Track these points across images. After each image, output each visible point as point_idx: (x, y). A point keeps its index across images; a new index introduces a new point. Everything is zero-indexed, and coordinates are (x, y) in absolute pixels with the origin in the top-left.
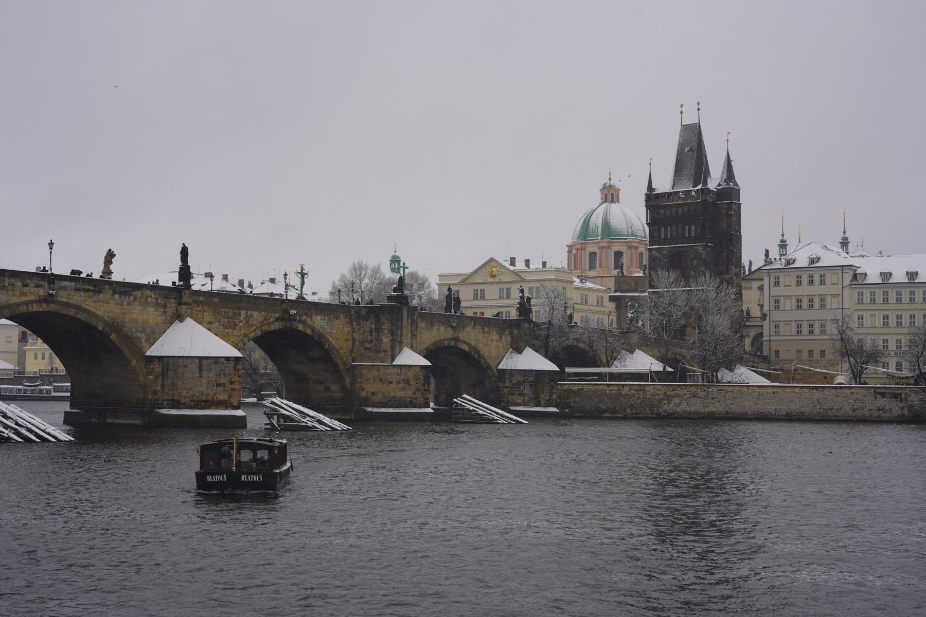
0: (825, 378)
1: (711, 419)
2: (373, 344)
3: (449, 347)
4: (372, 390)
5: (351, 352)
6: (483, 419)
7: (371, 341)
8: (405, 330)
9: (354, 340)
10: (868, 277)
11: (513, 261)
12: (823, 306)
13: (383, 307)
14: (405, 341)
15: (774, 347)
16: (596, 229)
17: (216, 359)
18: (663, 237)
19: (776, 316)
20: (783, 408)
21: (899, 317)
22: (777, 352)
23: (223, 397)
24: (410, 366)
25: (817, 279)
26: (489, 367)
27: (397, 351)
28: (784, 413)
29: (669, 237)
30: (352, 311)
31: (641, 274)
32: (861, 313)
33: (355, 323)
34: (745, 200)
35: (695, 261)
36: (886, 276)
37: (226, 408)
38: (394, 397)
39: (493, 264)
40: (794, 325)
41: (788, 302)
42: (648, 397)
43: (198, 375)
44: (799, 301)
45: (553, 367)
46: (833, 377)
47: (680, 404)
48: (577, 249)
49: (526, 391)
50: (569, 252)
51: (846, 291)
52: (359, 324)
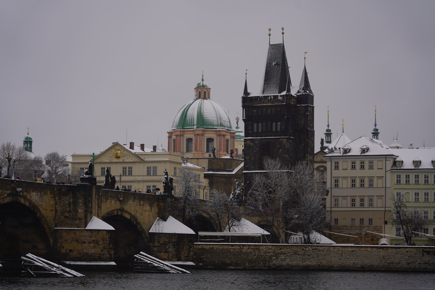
0: (372, 240)
1: (307, 270)
2: (71, 214)
3: (117, 215)
4: (70, 248)
5: (54, 219)
6: (158, 270)
7: (70, 212)
8: (93, 203)
9: (56, 210)
10: (404, 164)
11: (132, 145)
12: (371, 185)
13: (79, 186)
14: (94, 211)
15: (334, 216)
16: (192, 120)
18: (255, 130)
19: (336, 192)
20: (359, 262)
21: (426, 194)
22: (336, 220)
24: (99, 230)
25: (367, 165)
26: (143, 231)
27: (89, 219)
28: (360, 266)
29: (260, 130)
30: (55, 189)
31: (228, 157)
33: (57, 198)
34: (316, 104)
35: (281, 150)
36: (417, 163)
38: (87, 254)
39: (118, 147)
40: (349, 200)
41: (345, 181)
42: (262, 254)
44: (353, 181)
45: (190, 231)
46: (378, 240)
47: (285, 259)
48: (177, 136)
49: (170, 250)
50: (170, 137)
51: (388, 174)
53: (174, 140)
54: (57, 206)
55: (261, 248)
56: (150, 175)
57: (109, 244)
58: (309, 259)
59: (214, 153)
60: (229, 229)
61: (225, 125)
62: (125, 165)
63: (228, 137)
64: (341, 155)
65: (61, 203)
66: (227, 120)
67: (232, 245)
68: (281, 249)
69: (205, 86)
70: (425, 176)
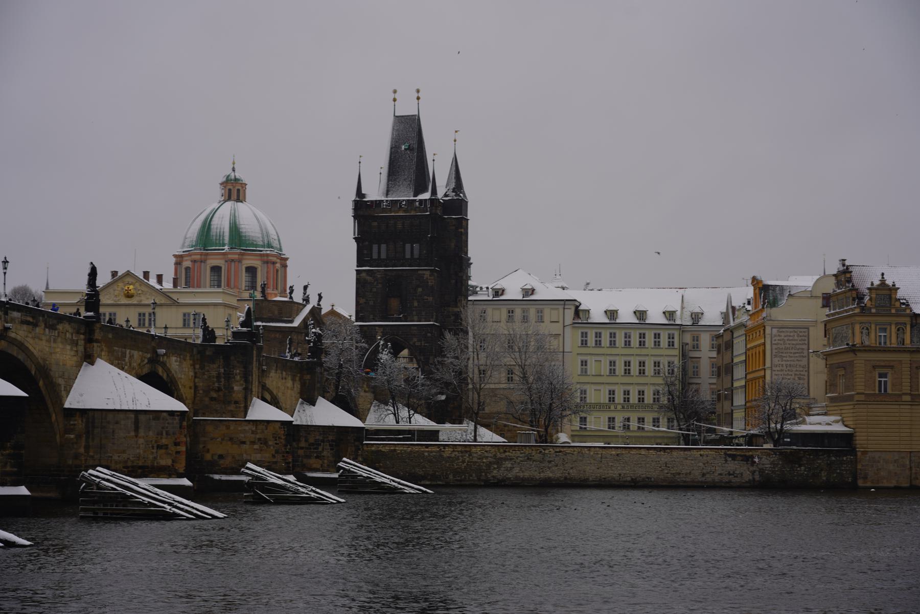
2: (221, 394)
4: (220, 452)
6: (383, 488)
7: (219, 390)
11: (146, 274)
16: (221, 235)
17: (157, 414)
23: (166, 462)
24: (268, 422)
28: (629, 479)
29: (383, 256)
30: (195, 350)
32: (584, 358)
35: (420, 290)
37: (170, 476)
43: (133, 434)
47: (512, 468)
48: (194, 261)
49: (325, 453)
50: (178, 264)
52: (202, 368)
53: (187, 269)
54: (197, 380)
55: (474, 450)
56: (189, 327)
57: (285, 446)
58: (549, 468)
59: (263, 292)
60: (410, 418)
61: (274, 245)
62: (142, 310)
63: (278, 265)
64: (490, 298)
65: (204, 374)
66: (276, 237)
67: (427, 446)
68: (505, 452)
69: (238, 180)
70: (626, 334)
